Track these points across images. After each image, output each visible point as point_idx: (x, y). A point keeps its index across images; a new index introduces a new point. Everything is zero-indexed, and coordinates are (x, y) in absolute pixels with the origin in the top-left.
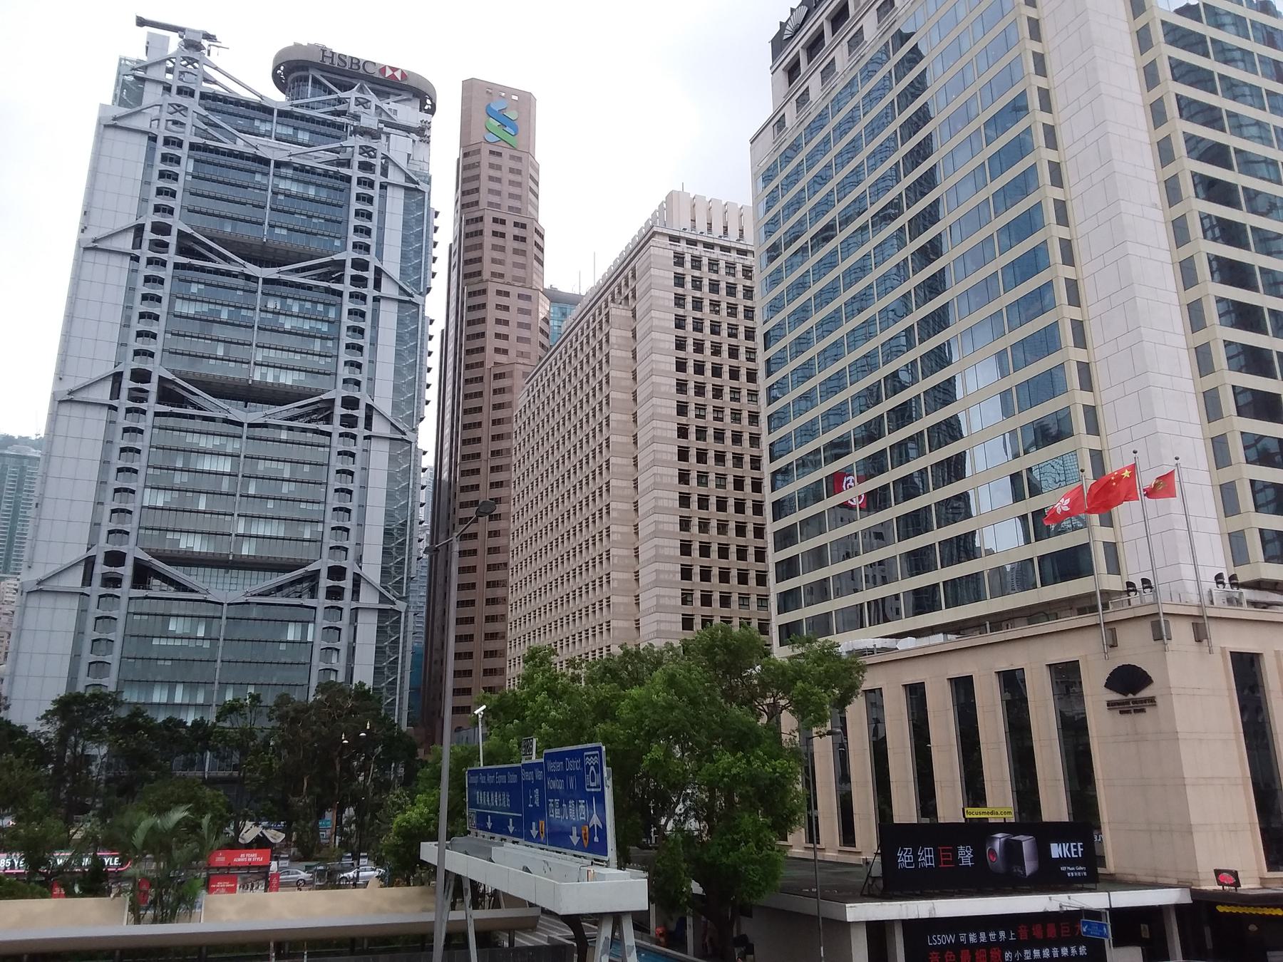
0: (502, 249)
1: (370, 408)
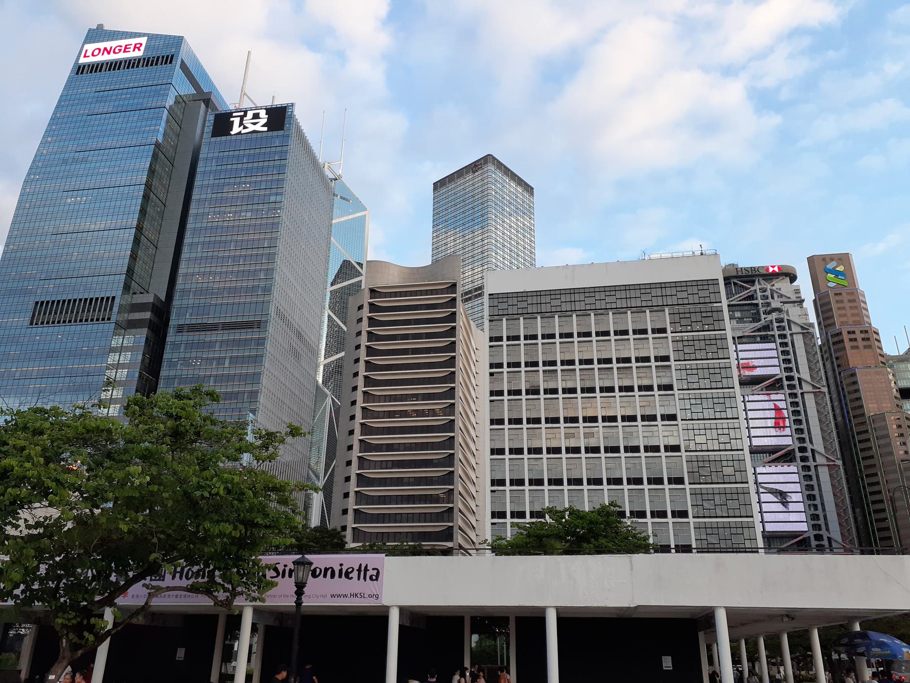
0: (857, 347)
1: (813, 451)
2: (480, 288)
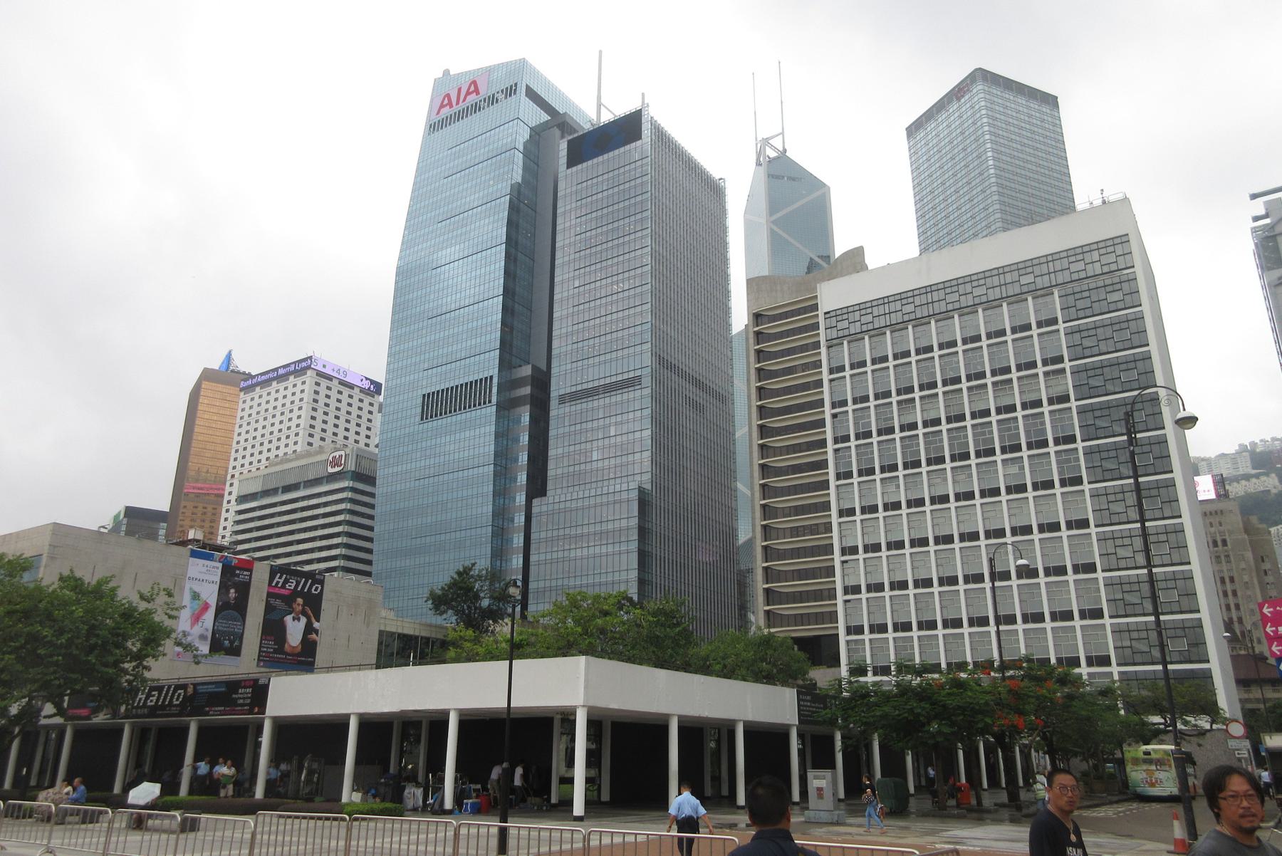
2: (815, 307)
